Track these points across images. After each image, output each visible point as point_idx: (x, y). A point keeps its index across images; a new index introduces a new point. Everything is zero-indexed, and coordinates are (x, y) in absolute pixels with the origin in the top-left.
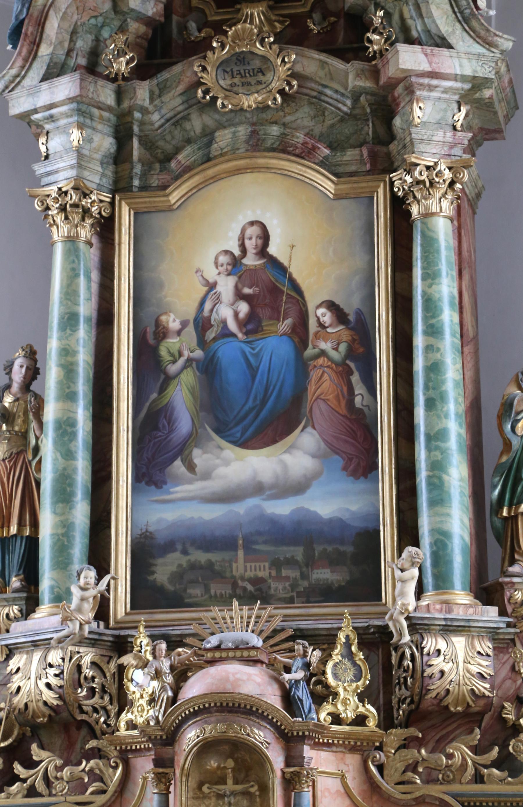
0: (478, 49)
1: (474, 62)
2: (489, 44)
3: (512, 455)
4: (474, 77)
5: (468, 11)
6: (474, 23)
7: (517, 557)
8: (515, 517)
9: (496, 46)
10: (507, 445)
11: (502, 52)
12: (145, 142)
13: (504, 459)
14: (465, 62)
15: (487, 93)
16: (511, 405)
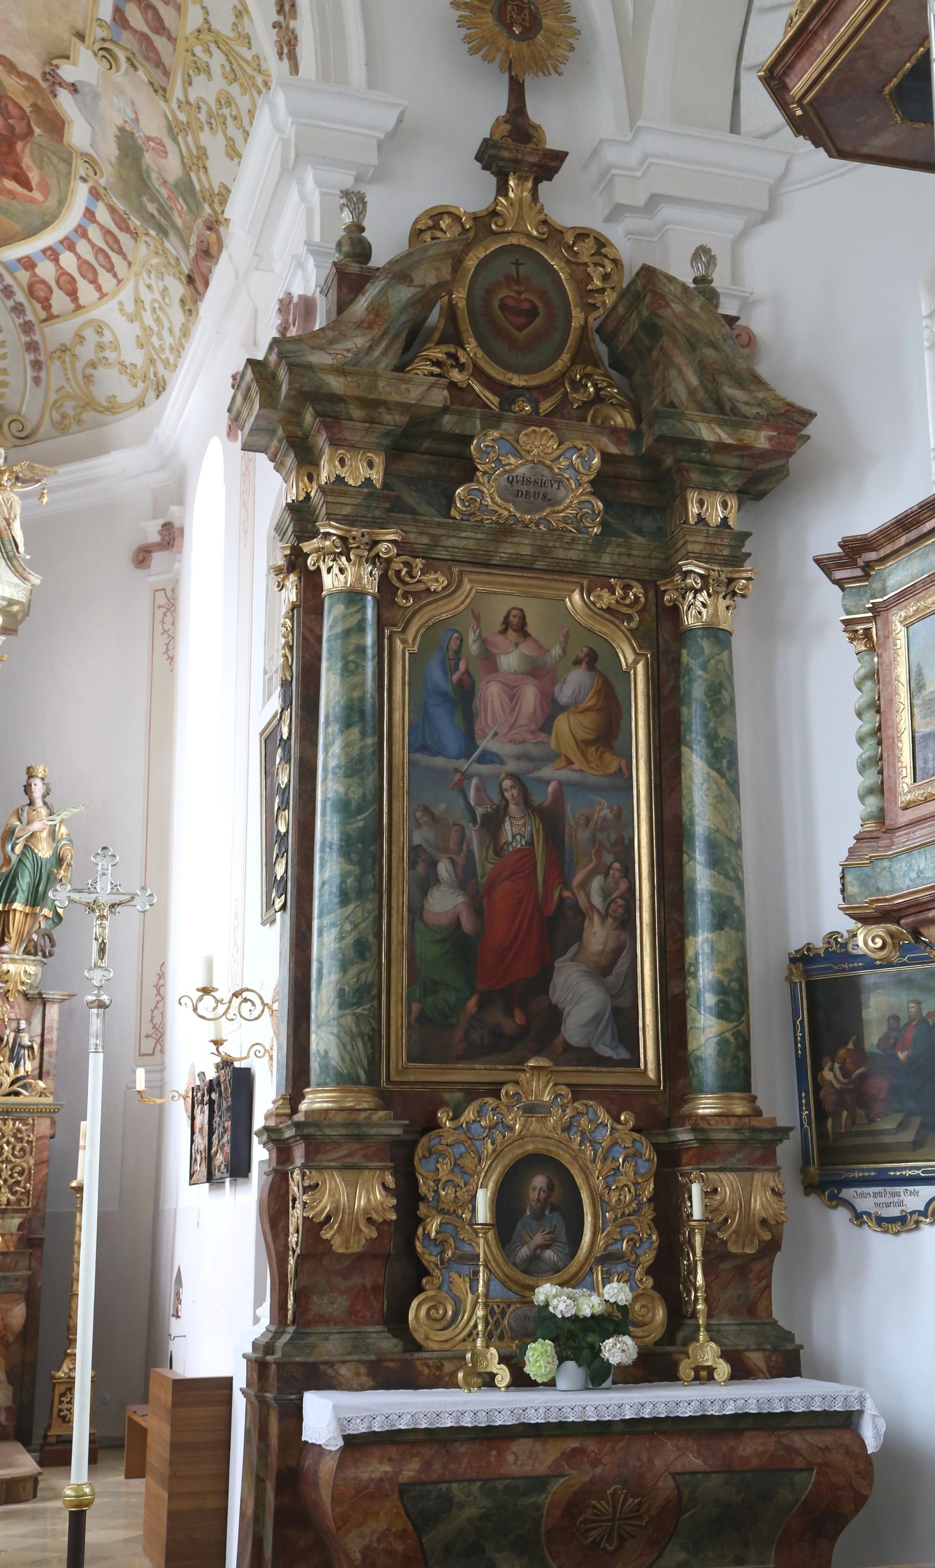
0: (16, 580)
1: (12, 588)
2: (24, 579)
3: (10, 867)
4: (11, 599)
5: (11, 554)
6: (15, 562)
7: (6, 939)
8: (8, 912)
9: (29, 581)
10: (8, 860)
11: (32, 585)
13: (4, 870)
14: (6, 587)
15: (15, 608)
16: (13, 832)
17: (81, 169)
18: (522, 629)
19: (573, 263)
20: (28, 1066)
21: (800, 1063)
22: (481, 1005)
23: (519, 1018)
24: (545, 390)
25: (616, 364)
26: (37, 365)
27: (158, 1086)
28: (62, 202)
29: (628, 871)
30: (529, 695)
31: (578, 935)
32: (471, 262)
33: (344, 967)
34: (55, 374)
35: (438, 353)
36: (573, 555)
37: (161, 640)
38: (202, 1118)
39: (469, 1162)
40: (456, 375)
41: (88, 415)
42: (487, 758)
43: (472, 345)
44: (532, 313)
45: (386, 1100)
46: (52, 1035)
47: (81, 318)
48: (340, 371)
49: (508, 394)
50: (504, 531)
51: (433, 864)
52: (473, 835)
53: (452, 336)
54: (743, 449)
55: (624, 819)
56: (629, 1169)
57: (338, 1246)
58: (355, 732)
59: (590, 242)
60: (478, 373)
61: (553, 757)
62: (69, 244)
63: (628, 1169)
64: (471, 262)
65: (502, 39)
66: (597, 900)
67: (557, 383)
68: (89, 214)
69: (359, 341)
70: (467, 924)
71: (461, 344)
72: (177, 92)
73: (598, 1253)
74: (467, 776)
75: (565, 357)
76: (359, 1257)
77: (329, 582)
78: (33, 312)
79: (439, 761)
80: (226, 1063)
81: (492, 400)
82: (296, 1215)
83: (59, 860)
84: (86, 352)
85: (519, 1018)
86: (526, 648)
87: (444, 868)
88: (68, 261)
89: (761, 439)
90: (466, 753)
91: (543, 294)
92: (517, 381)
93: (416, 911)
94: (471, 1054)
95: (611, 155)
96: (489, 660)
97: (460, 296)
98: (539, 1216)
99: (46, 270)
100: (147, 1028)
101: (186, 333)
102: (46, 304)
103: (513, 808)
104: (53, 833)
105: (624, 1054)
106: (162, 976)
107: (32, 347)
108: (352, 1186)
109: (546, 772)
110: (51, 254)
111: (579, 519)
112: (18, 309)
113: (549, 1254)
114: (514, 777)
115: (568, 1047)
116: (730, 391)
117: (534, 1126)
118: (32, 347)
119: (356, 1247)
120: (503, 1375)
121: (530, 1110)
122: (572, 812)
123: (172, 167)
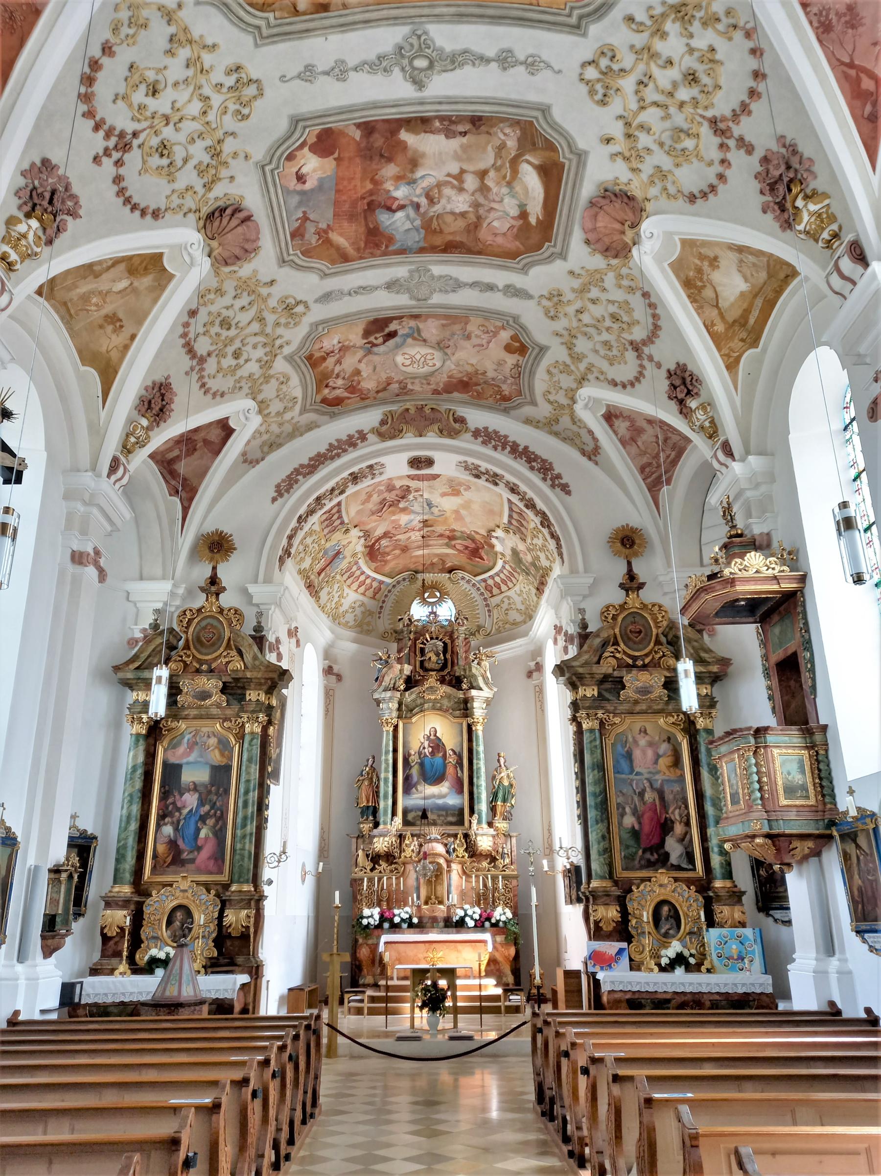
12: (406, 706)
17: (500, 556)
18: (645, 732)
19: (653, 615)
20: (507, 861)
21: (752, 867)
22: (644, 852)
23: (656, 856)
24: (647, 655)
25: (669, 643)
26: (489, 611)
27: (552, 867)
28: (495, 564)
29: (687, 807)
30: (650, 753)
31: (672, 829)
32: (620, 619)
33: (599, 843)
34: (495, 612)
35: (611, 649)
36: (660, 707)
37: (539, 704)
38: (567, 882)
39: (643, 902)
40: (618, 655)
41: (507, 626)
42: (638, 774)
43: (622, 645)
44: (640, 632)
45: (616, 883)
46: (514, 849)
47: (503, 595)
48: (581, 666)
49: (635, 658)
50: (636, 702)
51: (624, 808)
52: (636, 798)
53: (616, 643)
54: (710, 672)
55: (684, 790)
56: (695, 904)
57: (605, 929)
58: (596, 772)
59: (657, 608)
60: (625, 653)
61: (658, 772)
62: (497, 574)
63: (695, 904)
64: (620, 619)
65: (624, 550)
66: (678, 817)
67: (650, 653)
68: (503, 567)
69: (586, 657)
70: (637, 827)
71: (618, 645)
72: (529, 540)
73: (687, 930)
74: (632, 780)
75: (652, 644)
76: (611, 932)
77: (585, 726)
78: (487, 595)
79: (623, 776)
80: (572, 864)
81: (630, 661)
82: (592, 918)
83: (511, 785)
84: (505, 606)
85: (656, 856)
86: (647, 738)
87: (628, 810)
88: (497, 579)
89: (715, 669)
90: (631, 773)
91: (643, 626)
92: (637, 654)
93: (620, 824)
94: (642, 868)
95: (661, 579)
96: (635, 742)
97: (617, 631)
98: (667, 919)
99: (490, 582)
100: (546, 845)
101: (538, 603)
102: (491, 592)
103: (648, 789)
104: (508, 776)
105: (691, 867)
106: (550, 826)
107: (487, 605)
108: (607, 910)
109: (657, 777)
110: (492, 577)
111: (660, 697)
112: (482, 594)
113: (671, 932)
114: (648, 780)
115: (672, 865)
116: (703, 655)
117: (663, 890)
118: (487, 605)
119: (610, 928)
120: (656, 969)
121: (661, 886)
122: (667, 789)
123: (529, 558)
